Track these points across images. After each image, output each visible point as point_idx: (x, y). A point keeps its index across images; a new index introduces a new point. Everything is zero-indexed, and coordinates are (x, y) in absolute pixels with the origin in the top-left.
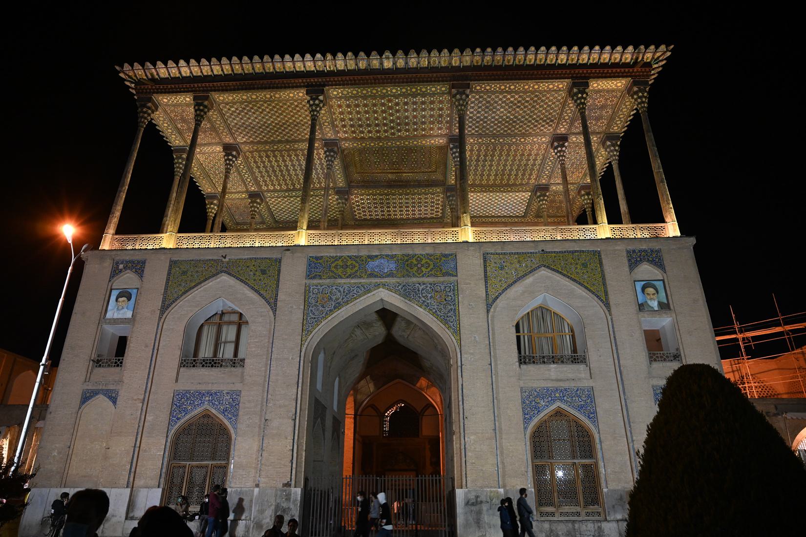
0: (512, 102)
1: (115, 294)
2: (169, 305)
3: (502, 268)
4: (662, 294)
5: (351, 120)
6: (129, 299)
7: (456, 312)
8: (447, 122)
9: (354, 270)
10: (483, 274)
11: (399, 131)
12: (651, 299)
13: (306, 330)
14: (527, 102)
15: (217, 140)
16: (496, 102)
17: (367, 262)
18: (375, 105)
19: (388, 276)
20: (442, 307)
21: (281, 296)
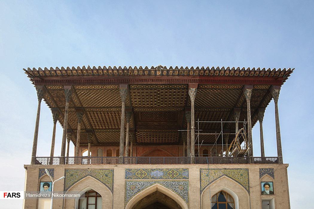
0: (216, 93)
1: (42, 184)
3: (207, 176)
4: (272, 188)
5: (139, 99)
6: (49, 186)
8: (185, 101)
11: (162, 104)
12: (267, 190)
13: (126, 201)
14: (224, 93)
15: (73, 105)
16: (209, 93)
18: (151, 93)
19: (159, 178)
20: (182, 192)
21: (115, 186)
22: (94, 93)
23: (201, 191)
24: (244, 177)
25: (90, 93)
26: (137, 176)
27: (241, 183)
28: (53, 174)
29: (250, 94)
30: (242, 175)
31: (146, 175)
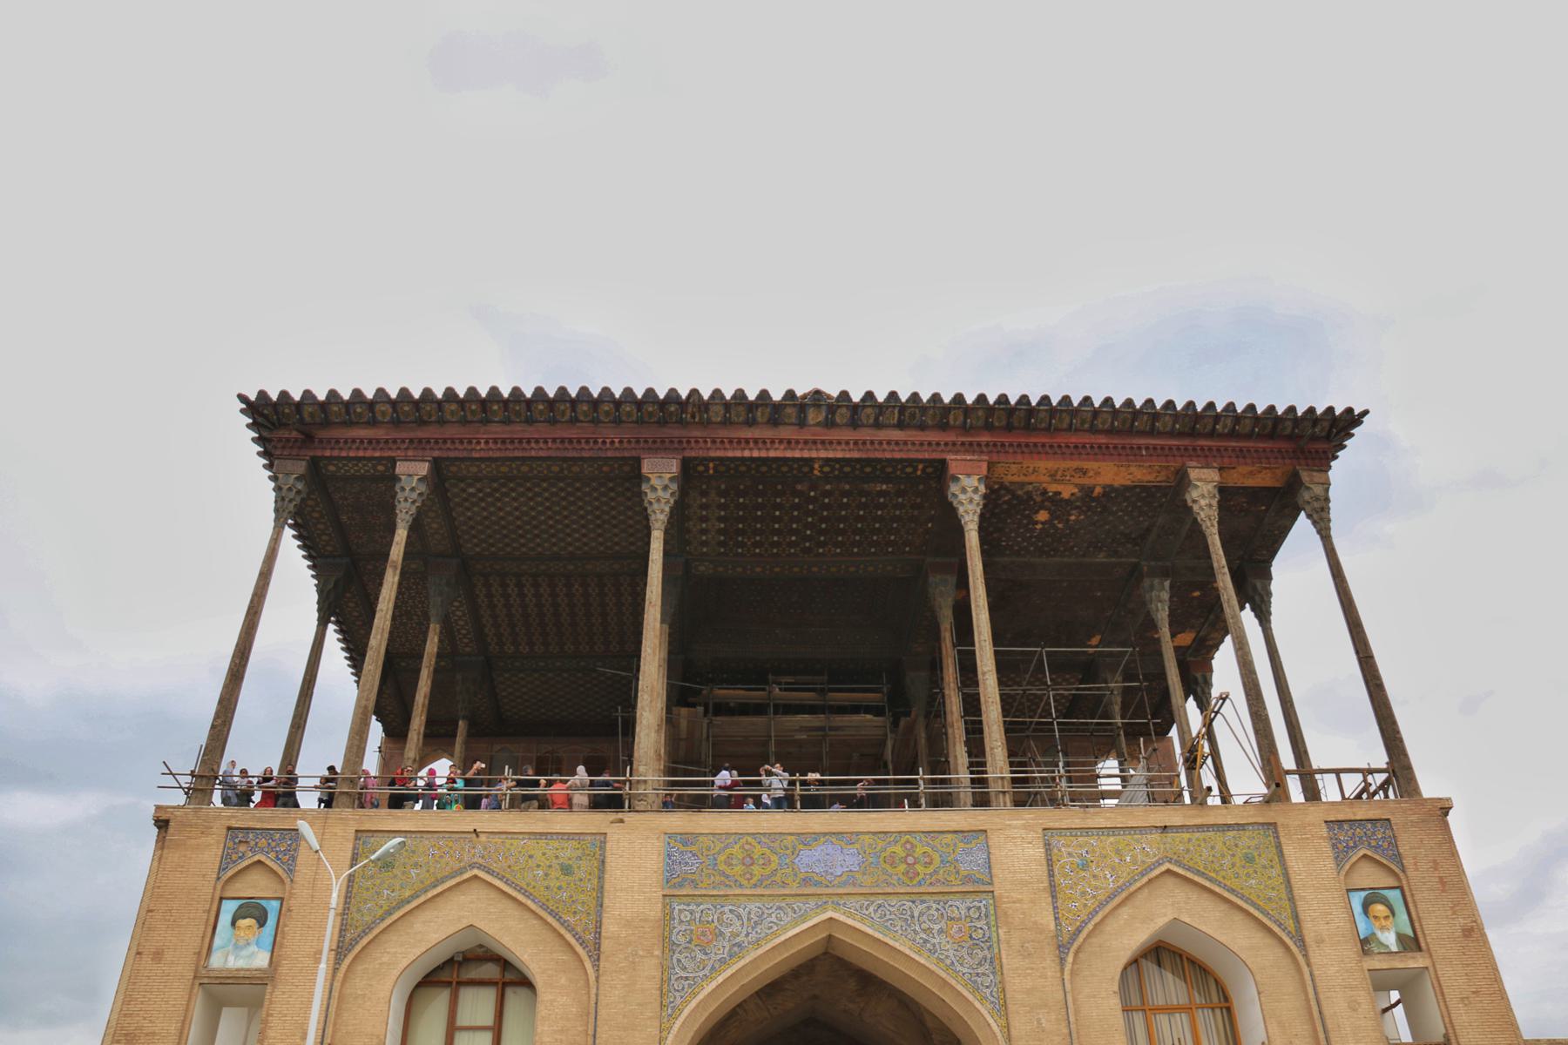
2: (355, 941)
3: (1085, 866)
4: (1403, 917)
6: (262, 922)
7: (995, 963)
9: (767, 871)
10: (1045, 877)
12: (1382, 928)
17: (795, 852)
19: (845, 884)
20: (964, 952)
21: (610, 927)
22: (522, 495)
23: (1062, 949)
24: (1264, 867)
25: (506, 495)
26: (728, 871)
27: (1254, 897)
28: (294, 859)
29: (1215, 502)
30: (1249, 859)
31: (774, 866)
